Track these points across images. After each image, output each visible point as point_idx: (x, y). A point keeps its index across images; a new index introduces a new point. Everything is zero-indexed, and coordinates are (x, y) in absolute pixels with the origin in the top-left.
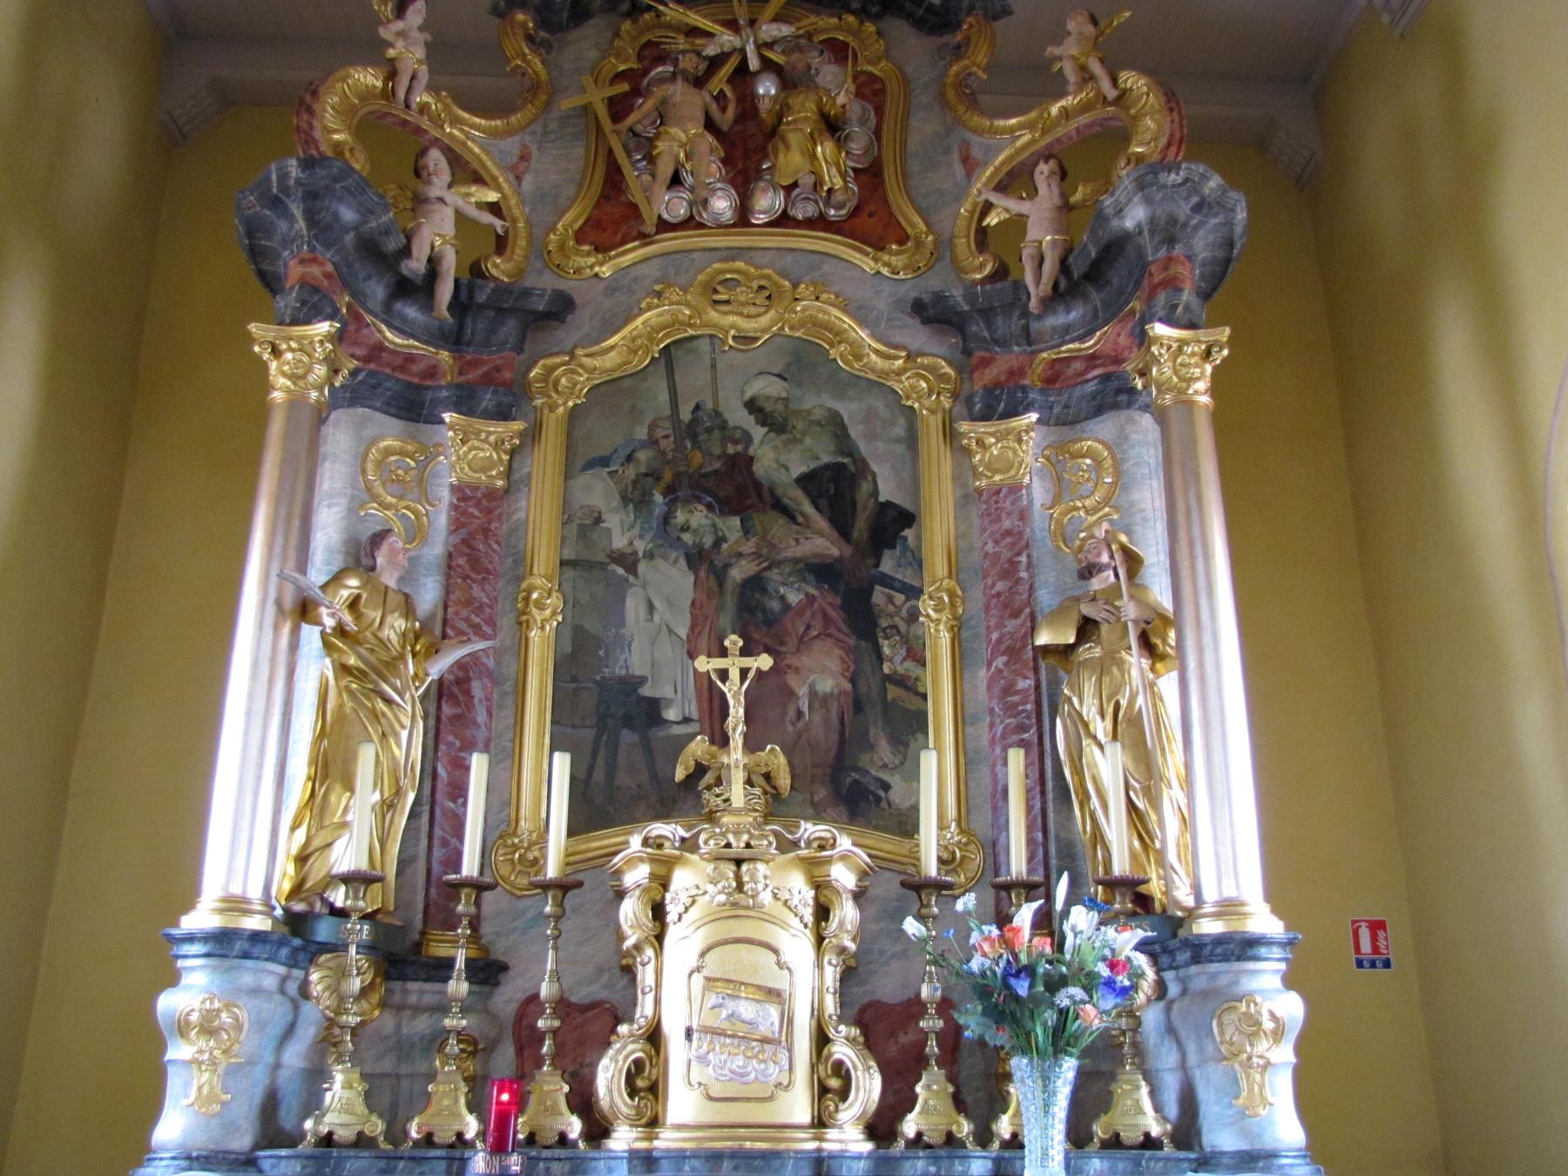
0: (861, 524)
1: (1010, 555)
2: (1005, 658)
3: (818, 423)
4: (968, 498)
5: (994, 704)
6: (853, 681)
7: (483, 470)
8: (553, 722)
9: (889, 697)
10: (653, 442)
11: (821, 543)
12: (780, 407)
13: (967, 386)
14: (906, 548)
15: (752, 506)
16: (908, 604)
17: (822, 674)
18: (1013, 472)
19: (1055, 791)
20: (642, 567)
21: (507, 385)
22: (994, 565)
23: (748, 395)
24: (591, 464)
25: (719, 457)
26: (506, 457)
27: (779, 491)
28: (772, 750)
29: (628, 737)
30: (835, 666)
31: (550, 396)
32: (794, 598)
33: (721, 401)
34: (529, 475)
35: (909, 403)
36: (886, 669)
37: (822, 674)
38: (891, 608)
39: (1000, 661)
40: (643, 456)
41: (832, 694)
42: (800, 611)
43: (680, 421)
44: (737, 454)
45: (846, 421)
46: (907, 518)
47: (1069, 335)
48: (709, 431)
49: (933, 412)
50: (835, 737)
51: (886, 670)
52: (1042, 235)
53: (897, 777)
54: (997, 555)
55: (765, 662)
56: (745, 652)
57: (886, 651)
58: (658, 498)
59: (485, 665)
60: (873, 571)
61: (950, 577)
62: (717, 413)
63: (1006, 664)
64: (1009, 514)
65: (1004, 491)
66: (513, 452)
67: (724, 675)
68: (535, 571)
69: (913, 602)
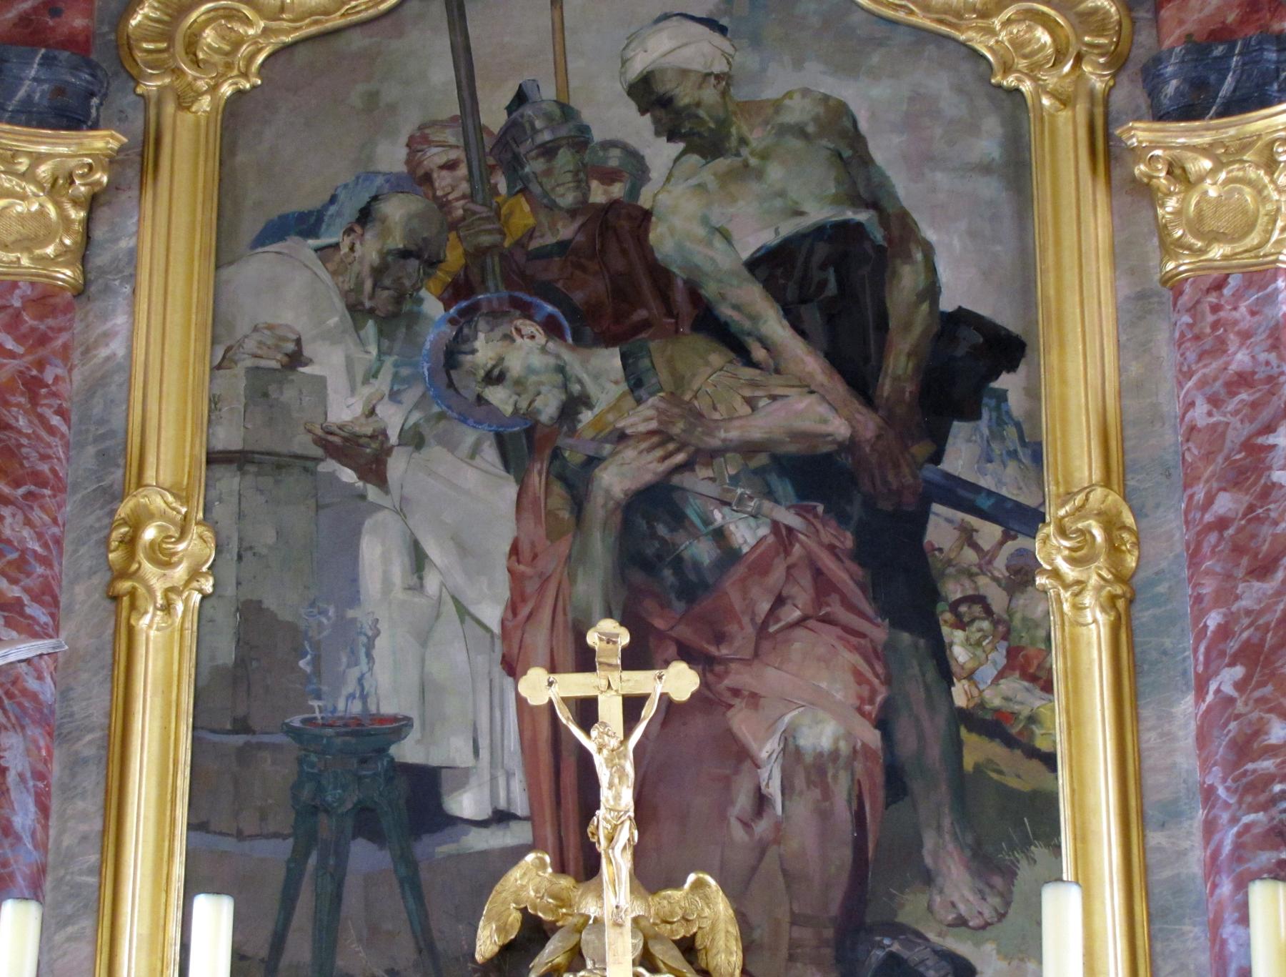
0: (899, 365)
1: (1248, 429)
2: (1238, 671)
3: (800, 131)
4: (1147, 299)
5: (1214, 777)
6: (883, 724)
7: (28, 243)
8: (191, 827)
9: (969, 762)
10: (418, 179)
11: (810, 408)
12: (710, 95)
13: (1145, 38)
14: (1002, 417)
15: (645, 325)
16: (1011, 546)
17: (812, 708)
18: (1253, 239)
20: (397, 466)
21: (79, 45)
22: (1209, 457)
23: (638, 65)
24: (276, 231)
25: (573, 213)
26: (77, 215)
27: (710, 290)
28: (699, 884)
29: (365, 857)
30: (841, 689)
31: (177, 72)
32: (746, 534)
33: (574, 83)
34: (133, 255)
35: (1010, 81)
36: (960, 695)
37: (812, 708)
38: (970, 556)
39: (1228, 677)
40: (396, 210)
41: (834, 755)
42: (761, 567)
43: (480, 129)
44: (613, 205)
45: (863, 126)
46: (1006, 349)
48: (548, 151)
49: (1065, 101)
50: (843, 855)
51: (960, 695)
53: (990, 947)
54: (1216, 432)
55: (680, 681)
56: (634, 659)
57: (960, 654)
58: (433, 307)
59: (34, 697)
60: (928, 472)
61: (1107, 483)
62: (567, 111)
63: (1241, 686)
64: (1245, 336)
65: (1233, 282)
66: (93, 203)
67: (586, 711)
68: (150, 476)
69: (1021, 542)
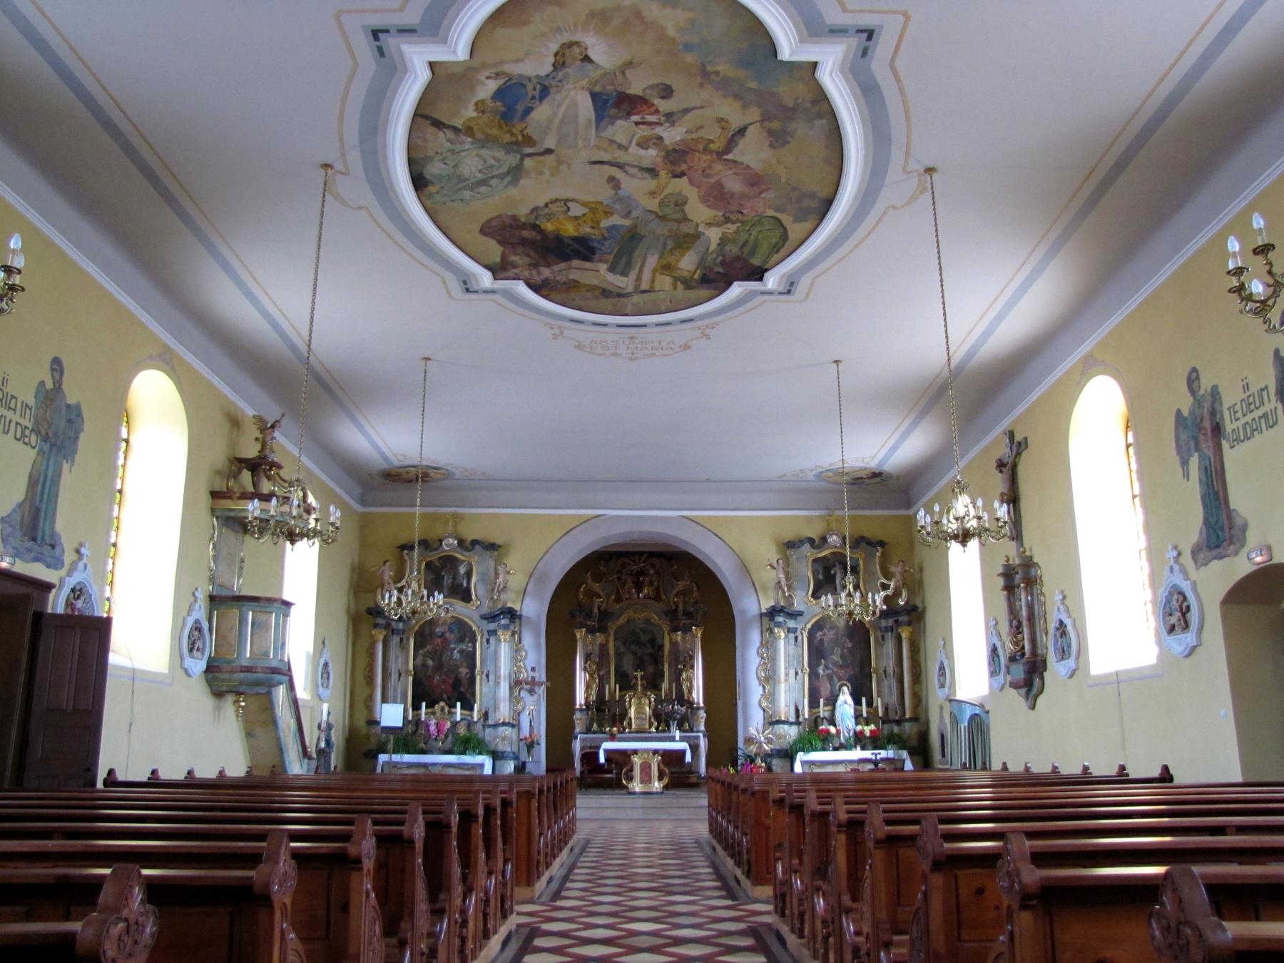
11: (650, 650)
17: (651, 669)
19: (679, 686)
37: (651, 669)
47: (684, 621)
52: (681, 608)
